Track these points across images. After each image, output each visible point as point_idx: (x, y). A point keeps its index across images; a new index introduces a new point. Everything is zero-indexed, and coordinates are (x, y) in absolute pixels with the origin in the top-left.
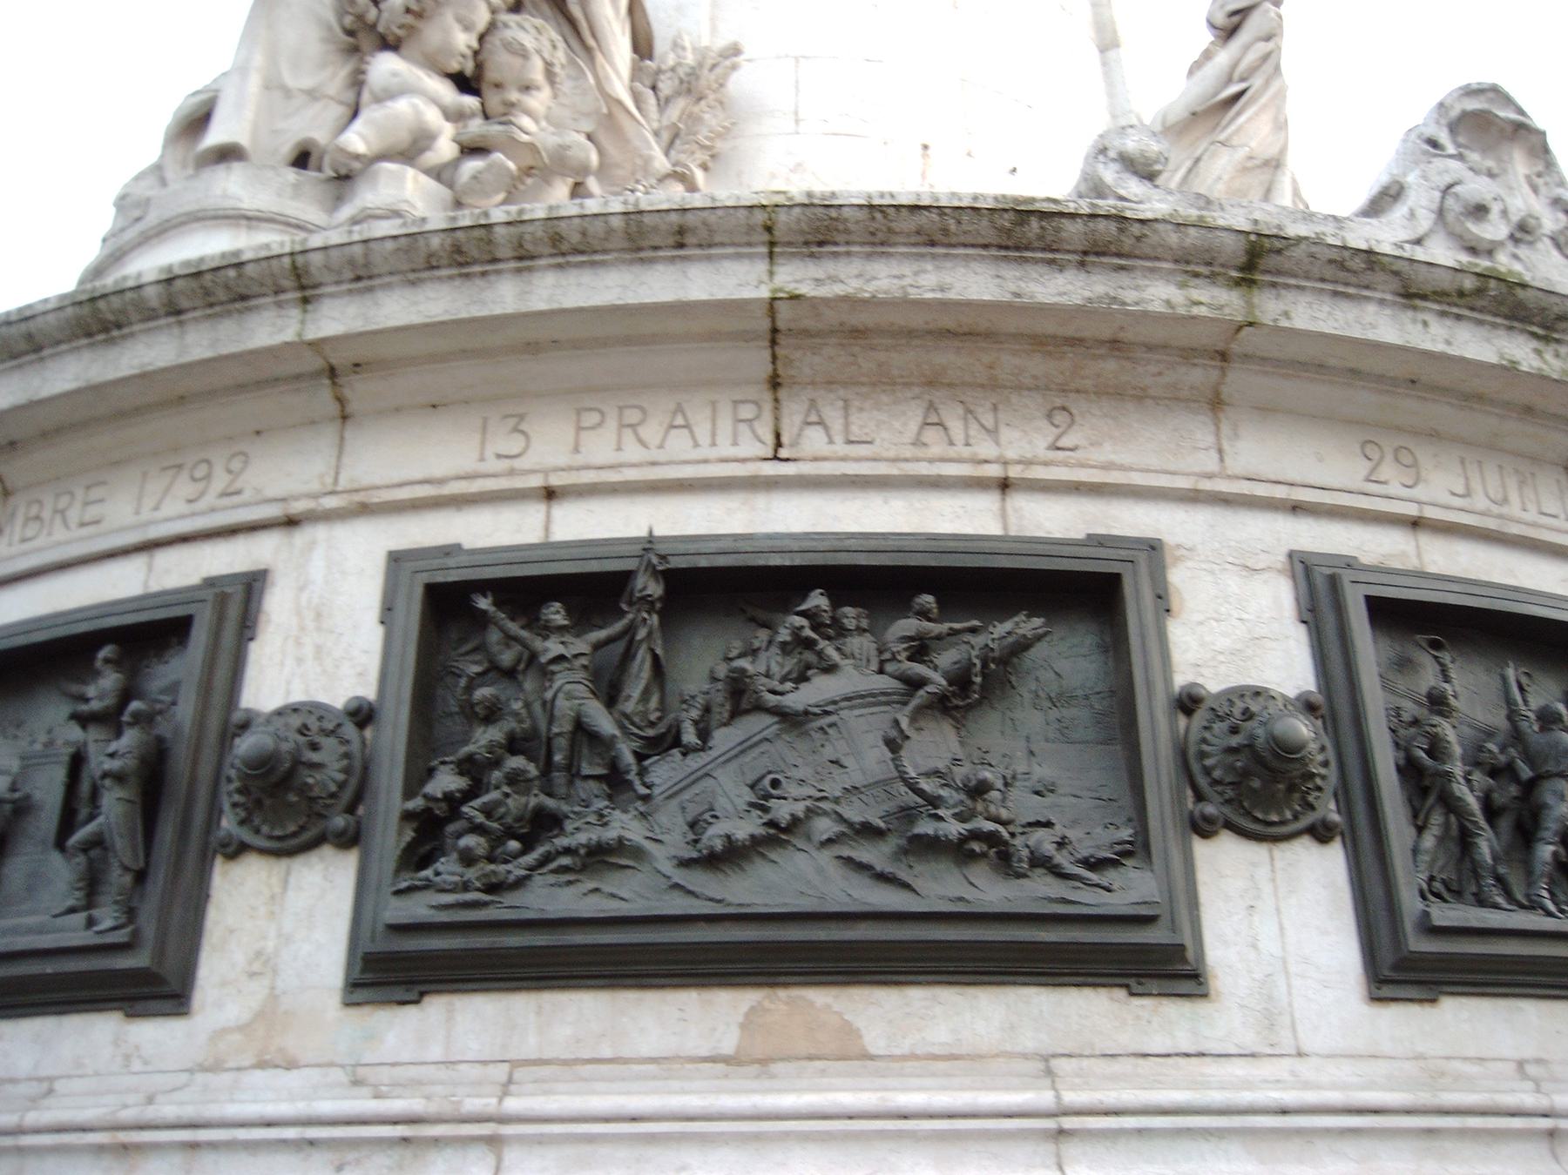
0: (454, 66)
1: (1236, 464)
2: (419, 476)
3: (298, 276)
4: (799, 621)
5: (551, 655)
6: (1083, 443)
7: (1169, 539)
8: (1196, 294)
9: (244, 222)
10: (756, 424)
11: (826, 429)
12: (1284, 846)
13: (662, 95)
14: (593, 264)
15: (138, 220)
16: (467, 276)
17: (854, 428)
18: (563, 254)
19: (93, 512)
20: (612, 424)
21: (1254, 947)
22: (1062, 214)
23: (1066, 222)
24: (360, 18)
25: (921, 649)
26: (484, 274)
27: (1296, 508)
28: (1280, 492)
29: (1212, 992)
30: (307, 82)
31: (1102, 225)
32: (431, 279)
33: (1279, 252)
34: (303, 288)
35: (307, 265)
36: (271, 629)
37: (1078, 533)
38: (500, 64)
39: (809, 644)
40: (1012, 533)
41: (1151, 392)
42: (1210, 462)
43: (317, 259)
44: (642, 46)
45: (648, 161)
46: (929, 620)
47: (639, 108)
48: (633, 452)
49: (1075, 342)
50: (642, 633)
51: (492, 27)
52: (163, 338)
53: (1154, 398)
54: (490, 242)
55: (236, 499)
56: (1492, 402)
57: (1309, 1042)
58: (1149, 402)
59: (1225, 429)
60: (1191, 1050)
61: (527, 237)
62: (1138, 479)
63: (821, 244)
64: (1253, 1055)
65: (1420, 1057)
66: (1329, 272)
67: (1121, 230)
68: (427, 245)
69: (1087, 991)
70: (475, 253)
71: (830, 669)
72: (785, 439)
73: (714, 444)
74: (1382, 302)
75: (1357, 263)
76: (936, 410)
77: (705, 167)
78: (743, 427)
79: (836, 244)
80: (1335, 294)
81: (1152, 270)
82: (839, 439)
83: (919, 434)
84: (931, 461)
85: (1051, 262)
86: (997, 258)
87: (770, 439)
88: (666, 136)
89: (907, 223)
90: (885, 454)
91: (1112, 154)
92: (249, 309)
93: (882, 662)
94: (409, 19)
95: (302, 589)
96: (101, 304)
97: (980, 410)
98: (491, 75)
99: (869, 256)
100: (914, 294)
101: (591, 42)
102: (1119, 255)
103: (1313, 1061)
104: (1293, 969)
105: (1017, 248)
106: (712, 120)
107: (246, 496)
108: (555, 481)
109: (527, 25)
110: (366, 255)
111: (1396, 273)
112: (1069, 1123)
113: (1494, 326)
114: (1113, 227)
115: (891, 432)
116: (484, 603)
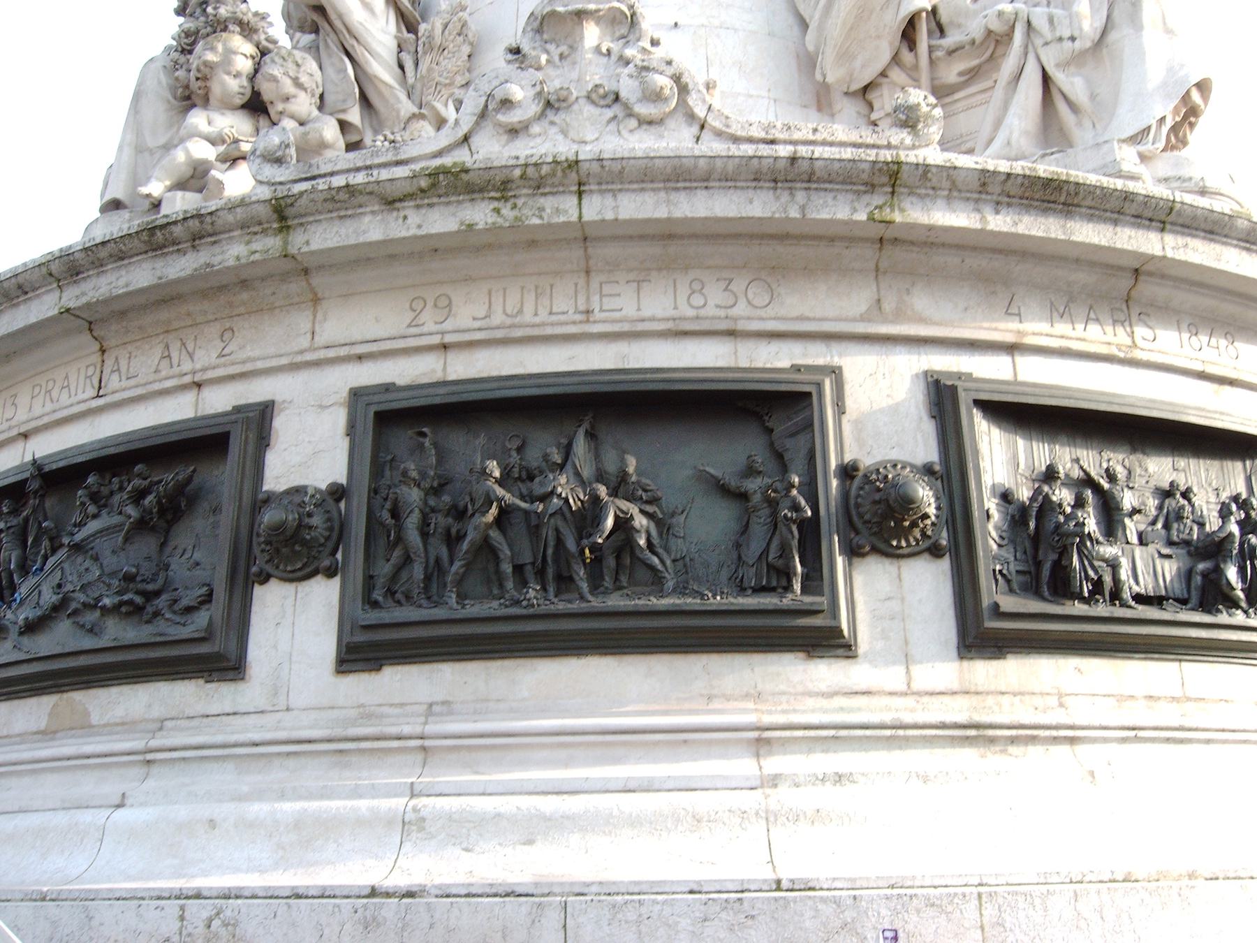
1: (321, 340)
7: (278, 398)
8: (256, 246)
12: (304, 583)
21: (275, 647)
22: (168, 224)
23: (173, 228)
27: (360, 358)
28: (343, 352)
29: (247, 677)
33: (292, 205)
41: (277, 304)
42: (305, 342)
49: (222, 288)
56: (500, 246)
57: (297, 700)
58: (277, 311)
59: (320, 316)
60: (231, 711)
62: (260, 365)
63: (77, 274)
64: (262, 712)
65: (362, 706)
66: (330, 206)
67: (202, 222)
69: (186, 682)
74: (373, 212)
75: (343, 196)
80: (341, 218)
81: (230, 238)
82: (124, 378)
85: (178, 250)
87: (97, 385)
89: (103, 253)
102: (210, 235)
103: (295, 712)
104: (294, 659)
105: (161, 249)
111: (371, 193)
112: (149, 757)
113: (459, 202)
114: (197, 222)
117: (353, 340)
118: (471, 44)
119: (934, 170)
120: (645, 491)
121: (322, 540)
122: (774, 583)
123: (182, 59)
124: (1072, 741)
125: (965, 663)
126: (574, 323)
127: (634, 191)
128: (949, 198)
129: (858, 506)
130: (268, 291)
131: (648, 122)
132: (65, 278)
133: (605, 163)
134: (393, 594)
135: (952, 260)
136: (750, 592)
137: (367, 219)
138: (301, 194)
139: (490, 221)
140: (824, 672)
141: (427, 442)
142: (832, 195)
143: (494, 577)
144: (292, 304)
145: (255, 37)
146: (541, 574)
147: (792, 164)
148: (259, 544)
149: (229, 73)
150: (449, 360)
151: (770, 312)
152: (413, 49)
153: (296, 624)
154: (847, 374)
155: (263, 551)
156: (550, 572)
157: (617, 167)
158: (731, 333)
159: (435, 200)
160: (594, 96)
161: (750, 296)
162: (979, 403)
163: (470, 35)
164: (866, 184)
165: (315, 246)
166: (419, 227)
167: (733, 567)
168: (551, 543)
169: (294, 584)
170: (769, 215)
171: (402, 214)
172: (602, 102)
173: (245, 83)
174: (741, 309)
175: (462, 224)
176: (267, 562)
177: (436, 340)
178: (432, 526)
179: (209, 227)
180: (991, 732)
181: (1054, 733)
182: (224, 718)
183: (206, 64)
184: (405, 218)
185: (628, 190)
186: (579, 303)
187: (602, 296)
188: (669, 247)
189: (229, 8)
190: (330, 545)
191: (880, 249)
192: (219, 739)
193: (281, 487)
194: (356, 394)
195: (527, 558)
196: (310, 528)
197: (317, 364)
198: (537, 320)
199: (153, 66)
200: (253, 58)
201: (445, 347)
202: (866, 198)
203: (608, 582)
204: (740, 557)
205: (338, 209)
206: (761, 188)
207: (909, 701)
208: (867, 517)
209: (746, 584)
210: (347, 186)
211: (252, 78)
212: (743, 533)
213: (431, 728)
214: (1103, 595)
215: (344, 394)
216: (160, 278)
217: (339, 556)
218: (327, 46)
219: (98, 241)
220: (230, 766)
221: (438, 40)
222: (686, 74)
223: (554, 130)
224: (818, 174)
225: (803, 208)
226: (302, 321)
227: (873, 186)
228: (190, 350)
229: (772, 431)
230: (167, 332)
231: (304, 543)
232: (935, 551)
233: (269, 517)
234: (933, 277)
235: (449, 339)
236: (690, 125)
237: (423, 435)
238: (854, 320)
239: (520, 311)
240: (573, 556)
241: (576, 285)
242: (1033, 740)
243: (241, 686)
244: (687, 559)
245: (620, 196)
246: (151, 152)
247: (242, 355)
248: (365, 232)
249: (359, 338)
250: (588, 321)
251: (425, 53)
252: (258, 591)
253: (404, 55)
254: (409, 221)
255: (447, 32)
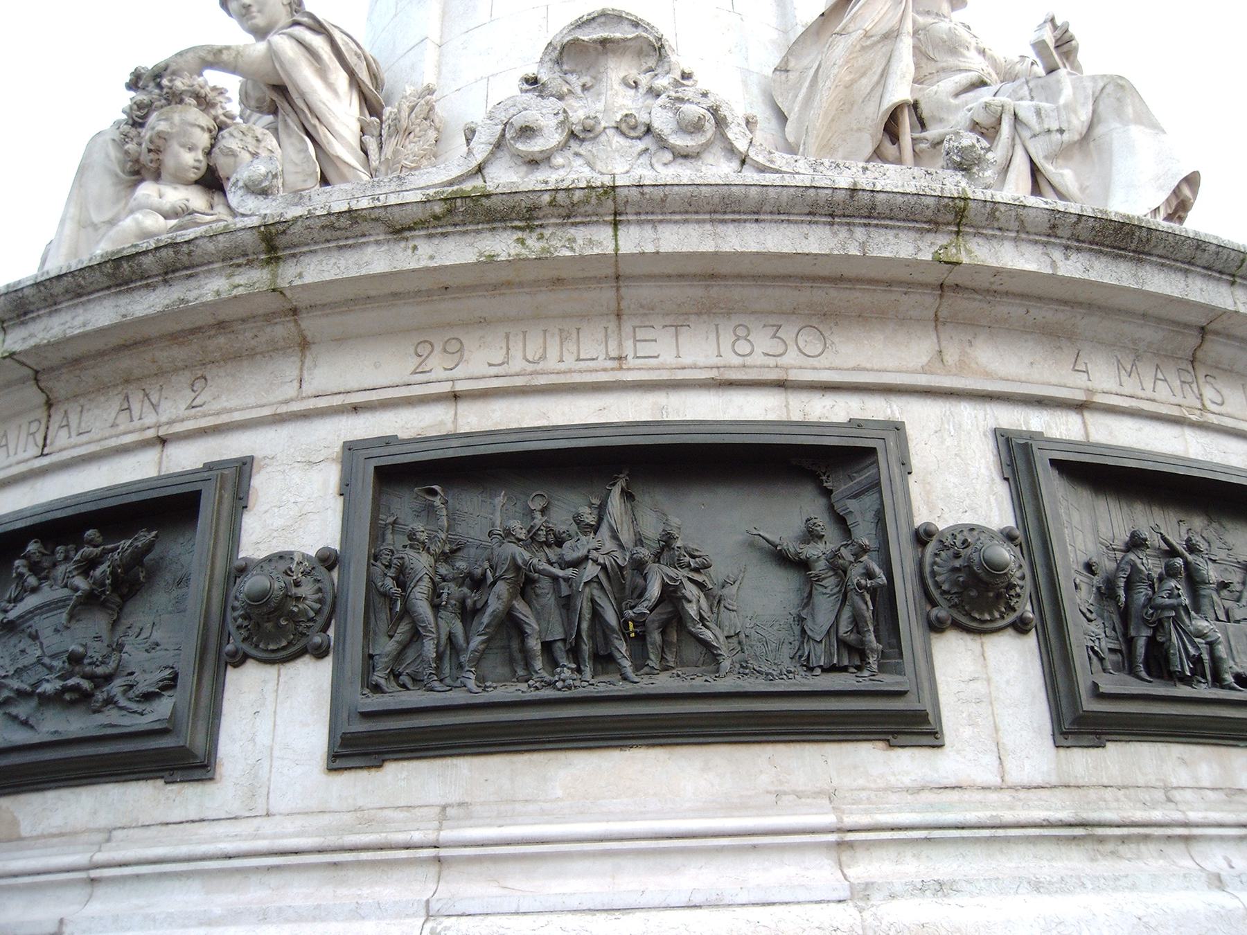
1: (308, 388)
7: (258, 454)
8: (237, 280)
21: (253, 740)
22: (138, 254)
23: (142, 258)
27: (356, 409)
28: (336, 401)
29: (217, 776)
31: (164, 253)
33: (284, 232)
41: (258, 350)
42: (291, 390)
49: (195, 331)
53: (261, 353)
56: (521, 284)
57: (277, 804)
58: (259, 356)
59: (308, 362)
62: (237, 417)
63: (25, 314)
64: (235, 818)
65: (360, 809)
66: (328, 234)
67: (176, 253)
69: (142, 783)
74: (377, 242)
75: (344, 222)
79: (32, 312)
80: (340, 248)
81: (210, 271)
85: (148, 286)
86: (116, 293)
87: (41, 443)
89: (58, 288)
91: (241, 184)
99: (50, 314)
100: (69, 333)
102: (187, 268)
103: (278, 818)
104: (276, 753)
105: (127, 283)
111: (377, 220)
112: (94, 874)
113: (478, 232)
114: (171, 252)
117: (348, 388)
118: (437, 130)
119: (1002, 208)
120: (693, 557)
121: (312, 614)
122: (846, 663)
123: (133, 132)
124: (1187, 839)
125: (1062, 751)
126: (605, 370)
127: (676, 222)
128: (1015, 240)
129: (934, 574)
130: (249, 335)
131: (683, 156)
132: (11, 319)
133: (646, 190)
134: (397, 676)
135: (1015, 310)
136: (818, 671)
137: (370, 250)
138: (296, 219)
139: (513, 252)
140: (905, 764)
141: (437, 501)
142: (893, 232)
143: (518, 656)
144: (275, 350)
145: (213, 112)
146: (574, 653)
147: (852, 197)
148: (235, 619)
149: (183, 146)
150: (460, 411)
151: (823, 361)
152: (376, 133)
153: (277, 716)
154: (911, 431)
155: (239, 627)
156: (586, 648)
157: (659, 193)
158: (782, 385)
159: (450, 229)
160: (624, 127)
161: (801, 344)
162: (1055, 463)
163: (437, 121)
164: (929, 222)
165: (309, 279)
166: (432, 258)
167: (797, 643)
168: (587, 615)
169: (276, 667)
170: (827, 252)
171: (411, 244)
172: (633, 134)
173: (201, 157)
174: (792, 358)
175: (481, 255)
176: (244, 640)
177: (446, 388)
178: (445, 596)
179: (185, 259)
180: (1100, 831)
181: (1169, 831)
182: (187, 825)
183: (160, 135)
184: (415, 248)
185: (669, 221)
186: (610, 349)
187: (636, 341)
188: (713, 290)
189: (186, 81)
190: (321, 620)
191: (941, 296)
192: (184, 850)
193: (261, 554)
194: (351, 449)
195: (557, 633)
196: (298, 599)
197: (305, 416)
198: (562, 367)
199: (100, 140)
200: (210, 131)
201: (456, 397)
202: (930, 237)
203: (654, 661)
204: (803, 632)
205: (338, 239)
206: (816, 223)
207: (1006, 796)
208: (945, 587)
209: (813, 663)
210: (350, 211)
211: (208, 153)
212: (807, 605)
213: (447, 835)
214: (1204, 676)
215: (337, 448)
216: (124, 316)
217: (331, 632)
218: (286, 125)
219: (53, 274)
220: (196, 884)
221: (404, 123)
222: (724, 106)
223: (580, 161)
224: (879, 209)
225: (863, 245)
226: (288, 368)
227: (937, 223)
229: (831, 492)
231: (292, 616)
232: (1021, 627)
233: (254, 583)
234: (996, 328)
235: (460, 386)
236: (730, 160)
237: (434, 493)
238: (915, 372)
239: (543, 357)
240: (614, 631)
241: (606, 328)
242: (1146, 838)
243: (209, 787)
244: (742, 636)
245: (660, 227)
246: (95, 227)
247: (216, 406)
248: (367, 263)
249: (356, 386)
250: (621, 368)
251: (390, 136)
252: (233, 677)
253: (367, 138)
254: (420, 251)
255: (413, 115)
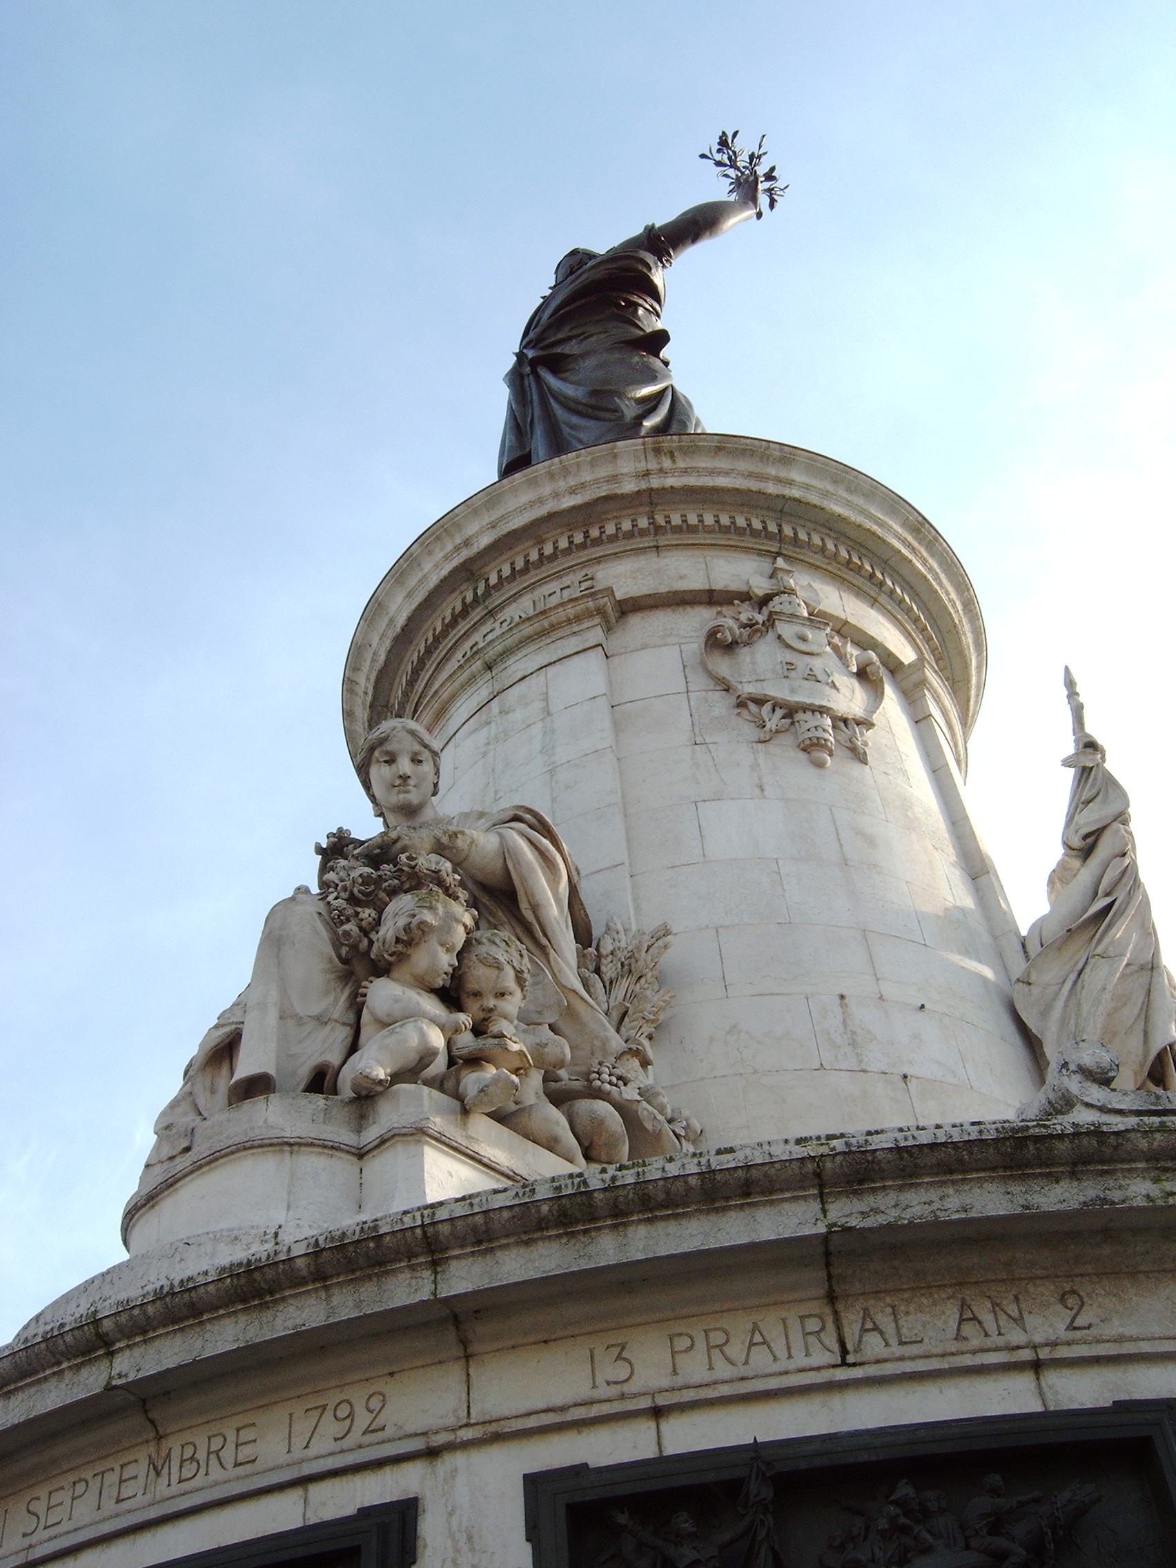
0: (439, 983)
2: (541, 1405)
3: (429, 1244)
4: (892, 1509)
5: (687, 1561)
6: (1095, 1321)
9: (287, 1148)
10: (822, 1335)
11: (882, 1333)
13: (606, 978)
14: (676, 1216)
15: (187, 1149)
16: (573, 1234)
17: (904, 1331)
18: (651, 1210)
19: (246, 1452)
20: (701, 1345)
22: (1051, 1136)
24: (354, 947)
25: (997, 1525)
26: (586, 1231)
30: (315, 1010)
32: (543, 1239)
34: (432, 1252)
35: (437, 1233)
36: (429, 1552)
37: (1105, 1401)
38: (479, 975)
39: (904, 1530)
40: (1052, 1409)
41: (1142, 1268)
43: (445, 1229)
44: (583, 935)
45: (605, 1042)
46: (999, 1496)
47: (588, 992)
48: (723, 1370)
50: (762, 1534)
51: (468, 944)
52: (312, 1301)
53: (1146, 1273)
54: (591, 1206)
55: (380, 1436)
61: (621, 1199)
62: (1146, 1347)
63: (861, 1182)
67: (1100, 1143)
68: (538, 1212)
70: (578, 1215)
71: (927, 1550)
72: (849, 1346)
73: (790, 1357)
76: (969, 1307)
77: (650, 1037)
78: (811, 1339)
81: (1130, 1170)
82: (893, 1341)
83: (959, 1329)
84: (974, 1352)
87: (836, 1347)
88: (615, 1015)
89: (930, 1159)
90: (935, 1351)
91: (1072, 1067)
92: (387, 1273)
93: (966, 1539)
94: (400, 947)
95: (450, 1514)
96: (257, 1275)
97: (1005, 1302)
98: (472, 985)
100: (943, 1216)
101: (544, 941)
102: (1102, 1162)
105: (1020, 1168)
106: (654, 998)
107: (389, 1432)
108: (661, 1401)
109: (497, 941)
110: (486, 1223)
115: (933, 1325)
116: (622, 1519)
123: (350, 911)
149: (442, 945)
179: (1108, 1151)
228: (1014, 1312)
230: (960, 1284)
246: (300, 1021)
